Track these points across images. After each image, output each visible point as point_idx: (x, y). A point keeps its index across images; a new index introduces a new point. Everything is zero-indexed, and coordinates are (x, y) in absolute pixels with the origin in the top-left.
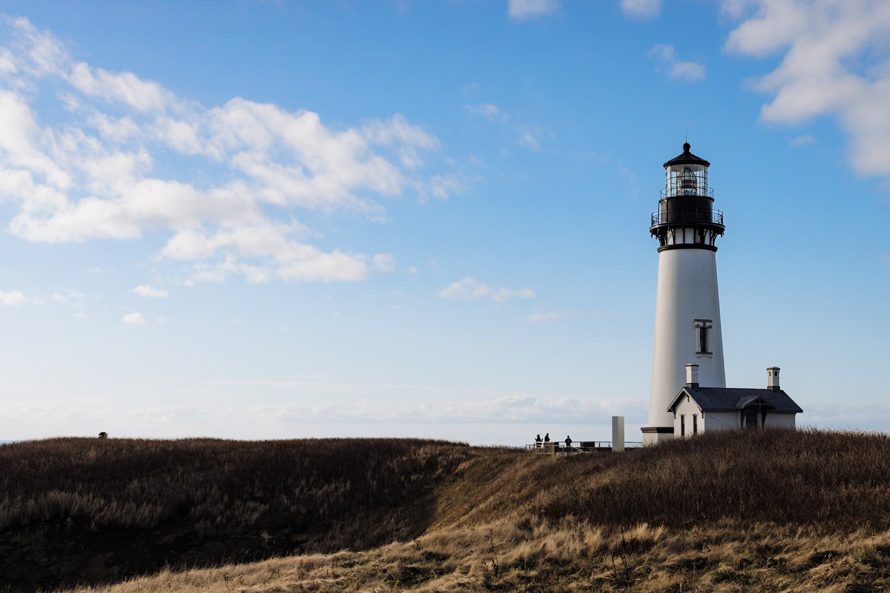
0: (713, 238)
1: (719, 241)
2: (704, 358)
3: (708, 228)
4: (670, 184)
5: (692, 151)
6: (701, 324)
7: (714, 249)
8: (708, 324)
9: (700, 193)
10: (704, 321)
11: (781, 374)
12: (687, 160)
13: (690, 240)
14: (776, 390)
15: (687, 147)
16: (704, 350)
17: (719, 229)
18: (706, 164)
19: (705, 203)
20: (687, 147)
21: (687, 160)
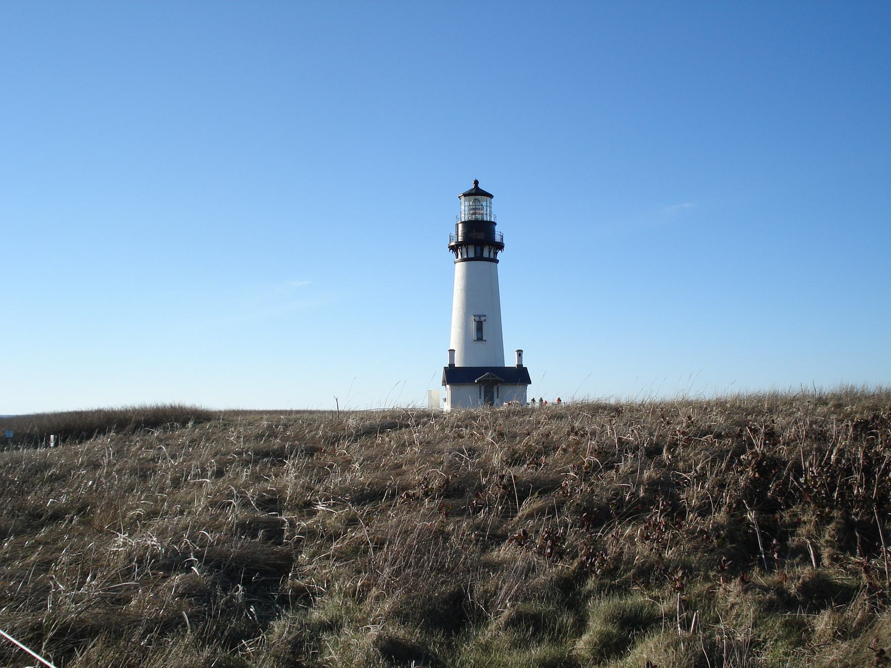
0: (496, 254)
1: (500, 255)
2: (480, 344)
3: (489, 245)
4: (463, 211)
5: (480, 186)
6: (477, 319)
7: (497, 261)
8: (483, 319)
9: (487, 218)
10: (480, 316)
11: (524, 355)
12: (477, 193)
13: (472, 255)
14: (520, 366)
15: (476, 182)
16: (480, 338)
17: (500, 246)
18: (491, 196)
19: (489, 227)
20: (476, 182)
21: (477, 193)
